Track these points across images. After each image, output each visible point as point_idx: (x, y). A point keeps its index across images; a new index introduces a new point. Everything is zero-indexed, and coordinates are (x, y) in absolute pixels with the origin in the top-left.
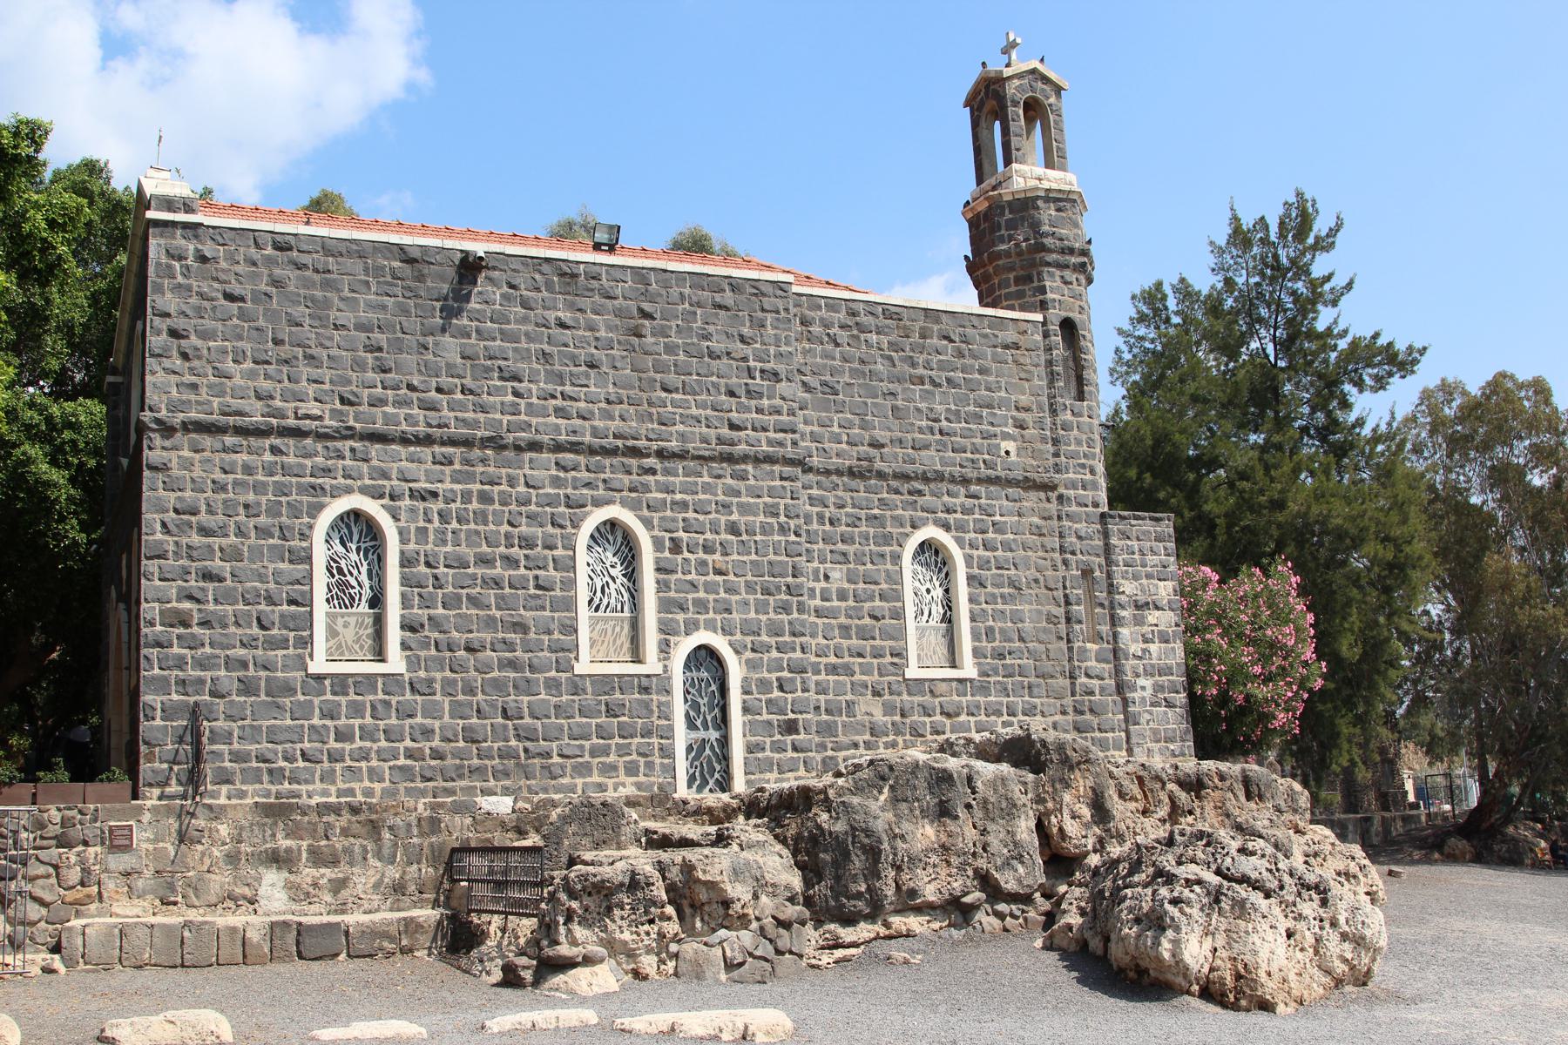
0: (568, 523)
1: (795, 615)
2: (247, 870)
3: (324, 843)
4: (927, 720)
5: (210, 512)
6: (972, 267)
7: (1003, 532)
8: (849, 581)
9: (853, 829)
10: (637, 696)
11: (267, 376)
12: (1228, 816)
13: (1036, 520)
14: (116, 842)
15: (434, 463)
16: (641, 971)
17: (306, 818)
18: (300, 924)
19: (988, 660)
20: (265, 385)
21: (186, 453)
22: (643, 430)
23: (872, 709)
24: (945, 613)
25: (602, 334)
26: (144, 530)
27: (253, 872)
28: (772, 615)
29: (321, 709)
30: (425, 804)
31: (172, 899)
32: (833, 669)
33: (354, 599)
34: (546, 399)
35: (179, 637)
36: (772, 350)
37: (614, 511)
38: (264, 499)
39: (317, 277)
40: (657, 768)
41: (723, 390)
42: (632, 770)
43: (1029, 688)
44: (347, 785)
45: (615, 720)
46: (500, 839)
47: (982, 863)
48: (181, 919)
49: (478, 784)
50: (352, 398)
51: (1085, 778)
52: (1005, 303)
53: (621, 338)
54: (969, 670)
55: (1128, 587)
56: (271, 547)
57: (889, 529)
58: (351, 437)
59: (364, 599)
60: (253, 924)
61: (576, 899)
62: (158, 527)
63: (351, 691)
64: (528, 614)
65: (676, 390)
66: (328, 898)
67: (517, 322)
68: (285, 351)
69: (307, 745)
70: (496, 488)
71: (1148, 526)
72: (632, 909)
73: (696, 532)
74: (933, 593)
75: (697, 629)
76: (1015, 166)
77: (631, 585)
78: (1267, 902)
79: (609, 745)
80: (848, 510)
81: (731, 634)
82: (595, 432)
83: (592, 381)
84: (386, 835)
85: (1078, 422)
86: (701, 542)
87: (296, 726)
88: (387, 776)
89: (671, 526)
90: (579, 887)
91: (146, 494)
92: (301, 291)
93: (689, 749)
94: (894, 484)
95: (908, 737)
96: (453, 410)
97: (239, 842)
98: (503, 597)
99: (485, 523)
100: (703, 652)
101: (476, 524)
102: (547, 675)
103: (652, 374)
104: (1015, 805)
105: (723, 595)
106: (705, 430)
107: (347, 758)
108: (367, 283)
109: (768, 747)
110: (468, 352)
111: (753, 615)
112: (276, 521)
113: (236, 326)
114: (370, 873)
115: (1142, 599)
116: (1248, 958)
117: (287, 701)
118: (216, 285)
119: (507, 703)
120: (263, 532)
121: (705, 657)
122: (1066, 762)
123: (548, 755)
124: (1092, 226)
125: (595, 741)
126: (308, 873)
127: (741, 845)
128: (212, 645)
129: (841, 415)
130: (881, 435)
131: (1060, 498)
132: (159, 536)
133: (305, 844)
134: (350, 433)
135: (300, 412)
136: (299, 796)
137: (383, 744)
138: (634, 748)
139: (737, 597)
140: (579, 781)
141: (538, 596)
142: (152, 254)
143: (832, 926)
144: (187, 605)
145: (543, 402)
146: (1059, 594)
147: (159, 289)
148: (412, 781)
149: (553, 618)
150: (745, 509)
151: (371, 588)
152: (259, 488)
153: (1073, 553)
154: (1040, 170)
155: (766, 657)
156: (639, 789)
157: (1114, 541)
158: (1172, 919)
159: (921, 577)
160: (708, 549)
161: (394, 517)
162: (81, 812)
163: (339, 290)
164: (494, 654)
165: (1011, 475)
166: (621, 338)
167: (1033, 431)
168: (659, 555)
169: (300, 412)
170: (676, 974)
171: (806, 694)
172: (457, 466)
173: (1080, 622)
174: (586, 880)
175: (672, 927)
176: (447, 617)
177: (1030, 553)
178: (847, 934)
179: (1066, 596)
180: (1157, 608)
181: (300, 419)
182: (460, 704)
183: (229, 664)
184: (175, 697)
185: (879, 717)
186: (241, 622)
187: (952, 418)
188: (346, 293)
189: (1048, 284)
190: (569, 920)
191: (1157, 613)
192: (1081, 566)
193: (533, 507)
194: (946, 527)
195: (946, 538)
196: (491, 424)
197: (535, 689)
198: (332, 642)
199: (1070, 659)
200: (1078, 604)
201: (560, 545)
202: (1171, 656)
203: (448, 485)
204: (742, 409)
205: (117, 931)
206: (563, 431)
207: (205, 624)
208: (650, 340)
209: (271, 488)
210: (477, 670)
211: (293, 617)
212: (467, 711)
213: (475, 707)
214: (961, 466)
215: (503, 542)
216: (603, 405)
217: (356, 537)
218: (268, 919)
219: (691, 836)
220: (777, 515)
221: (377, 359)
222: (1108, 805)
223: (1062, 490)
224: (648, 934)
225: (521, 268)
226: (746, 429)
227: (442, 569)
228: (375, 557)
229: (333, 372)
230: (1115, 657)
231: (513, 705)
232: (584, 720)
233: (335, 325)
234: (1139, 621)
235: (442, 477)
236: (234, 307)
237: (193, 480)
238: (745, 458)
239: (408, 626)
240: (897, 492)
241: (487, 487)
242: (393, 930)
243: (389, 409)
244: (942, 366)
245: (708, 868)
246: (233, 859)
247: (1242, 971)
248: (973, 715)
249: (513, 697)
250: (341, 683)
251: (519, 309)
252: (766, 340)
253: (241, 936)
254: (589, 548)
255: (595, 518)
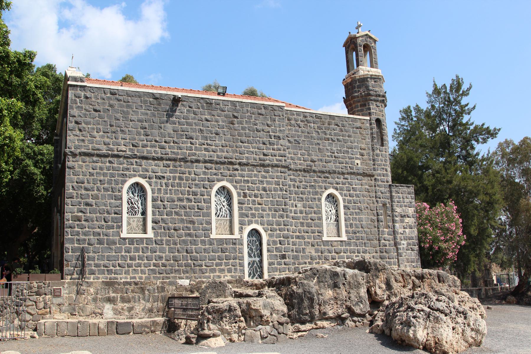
0: (209, 187)
1: (285, 219)
2: (100, 304)
3: (125, 295)
4: (330, 254)
5: (88, 183)
6: (345, 101)
7: (356, 191)
8: (303, 207)
9: (305, 291)
10: (232, 246)
11: (108, 137)
12: (432, 288)
13: (367, 187)
14: (56, 294)
15: (163, 167)
16: (232, 339)
17: (120, 286)
18: (117, 322)
19: (351, 234)
20: (107, 140)
21: (80, 163)
22: (234, 156)
23: (311, 251)
24: (336, 218)
25: (220, 123)
26: (66, 189)
27: (101, 304)
28: (277, 219)
29: (125, 249)
30: (160, 282)
31: (74, 313)
32: (298, 237)
33: (136, 212)
34: (201, 145)
35: (77, 225)
36: (278, 129)
37: (224, 183)
38: (106, 178)
39: (125, 104)
40: (238, 270)
41: (261, 142)
42: (230, 271)
43: (365, 244)
44: (133, 275)
45: (224, 254)
46: (185, 294)
47: (348, 303)
48: (77, 320)
49: (178, 275)
50: (136, 145)
51: (383, 275)
52: (357, 113)
53: (227, 125)
54: (344, 238)
55: (398, 210)
56: (109, 195)
57: (317, 190)
58: (136, 158)
59: (139, 212)
60: (101, 322)
61: (210, 315)
62: (71, 188)
63: (135, 243)
64: (195, 218)
65: (245, 142)
66: (127, 313)
67: (192, 119)
68: (114, 129)
69: (120, 262)
70: (184, 175)
71: (405, 189)
72: (230, 318)
73: (252, 190)
74: (332, 211)
75: (252, 223)
76: (360, 67)
77: (230, 208)
78: (446, 317)
79: (222, 263)
80: (303, 183)
81: (264, 225)
82: (218, 157)
83: (217, 139)
84: (147, 292)
85: (381, 154)
86: (253, 194)
87: (117, 255)
88: (147, 272)
89: (243, 188)
90: (211, 310)
91: (67, 177)
92: (119, 109)
93: (249, 264)
94: (319, 174)
95: (323, 260)
96: (170, 149)
97: (97, 294)
98: (186, 212)
99: (181, 187)
100: (254, 231)
101: (178, 187)
102: (201, 239)
103: (237, 137)
104: (360, 284)
105: (261, 212)
106: (255, 156)
107: (134, 266)
108: (142, 106)
109: (276, 263)
110: (175, 129)
111: (271, 219)
112: (110, 186)
113: (98, 120)
114: (141, 305)
115: (403, 214)
116: (439, 337)
117: (114, 247)
118: (91, 106)
119: (187, 248)
120: (106, 190)
121: (255, 233)
122: (377, 269)
123: (201, 266)
124: (386, 87)
125: (217, 261)
126: (120, 305)
127: (266, 297)
128: (88, 228)
129: (301, 151)
130: (315, 158)
131: (375, 179)
132: (71, 191)
133: (119, 295)
134: (135, 157)
135: (119, 149)
136: (117, 279)
137: (146, 261)
138: (230, 263)
139: (266, 213)
140: (212, 275)
141: (198, 212)
142: (69, 96)
143: (297, 325)
144: (80, 214)
145: (200, 146)
146: (375, 212)
147: (72, 108)
148: (156, 274)
149: (203, 219)
150: (268, 183)
151: (142, 209)
152: (105, 175)
153: (380, 198)
154: (369, 68)
155: (275, 233)
156: (232, 277)
157: (393, 194)
158: (413, 323)
159: (328, 206)
160: (256, 196)
161: (150, 185)
162: (44, 284)
163: (132, 108)
164: (183, 231)
165: (359, 172)
166: (227, 125)
167: (366, 157)
168: (239, 198)
169: (119, 149)
170: (244, 340)
171: (289, 246)
172: (171, 168)
173: (382, 222)
174: (214, 308)
175: (243, 325)
176: (168, 219)
177: (365, 198)
178: (302, 327)
179: (377, 213)
180: (408, 217)
181: (119, 151)
182: (172, 248)
183: (94, 234)
184: (76, 245)
185: (314, 254)
186: (98, 220)
187: (339, 152)
188: (134, 109)
189: (371, 107)
190: (208, 322)
191: (408, 219)
192: (382, 203)
193: (197, 182)
194: (337, 189)
195: (336, 193)
196: (183, 154)
197: (197, 243)
198: (129, 227)
199: (379, 234)
200: (381, 216)
201: (206, 194)
202: (413, 233)
203: (168, 174)
204: (268, 149)
205: (56, 324)
206: (207, 156)
207: (86, 220)
208: (236, 125)
209: (109, 175)
210: (177, 237)
211: (116, 218)
212: (174, 251)
213: (177, 249)
214: (342, 168)
215: (187, 194)
216: (221, 147)
217: (137, 192)
218: (107, 321)
219: (249, 293)
220: (279, 185)
221: (144, 131)
222: (391, 284)
223: (376, 177)
224: (235, 327)
225: (193, 101)
226: (269, 156)
227: (166, 203)
228: (143, 198)
229: (130, 136)
230: (394, 233)
231: (190, 249)
232: (214, 254)
233: (130, 120)
234: (402, 221)
235: (166, 171)
236: (97, 114)
237: (83, 172)
238: (268, 166)
239: (154, 222)
240: (320, 177)
241: (181, 175)
242: (149, 325)
243: (149, 148)
244: (335, 135)
245: (255, 304)
246: (95, 300)
247: (437, 341)
248: (345, 253)
249: (189, 246)
250: (132, 241)
251: (192, 115)
252: (276, 126)
253: (97, 326)
254: (216, 195)
255: (218, 185)
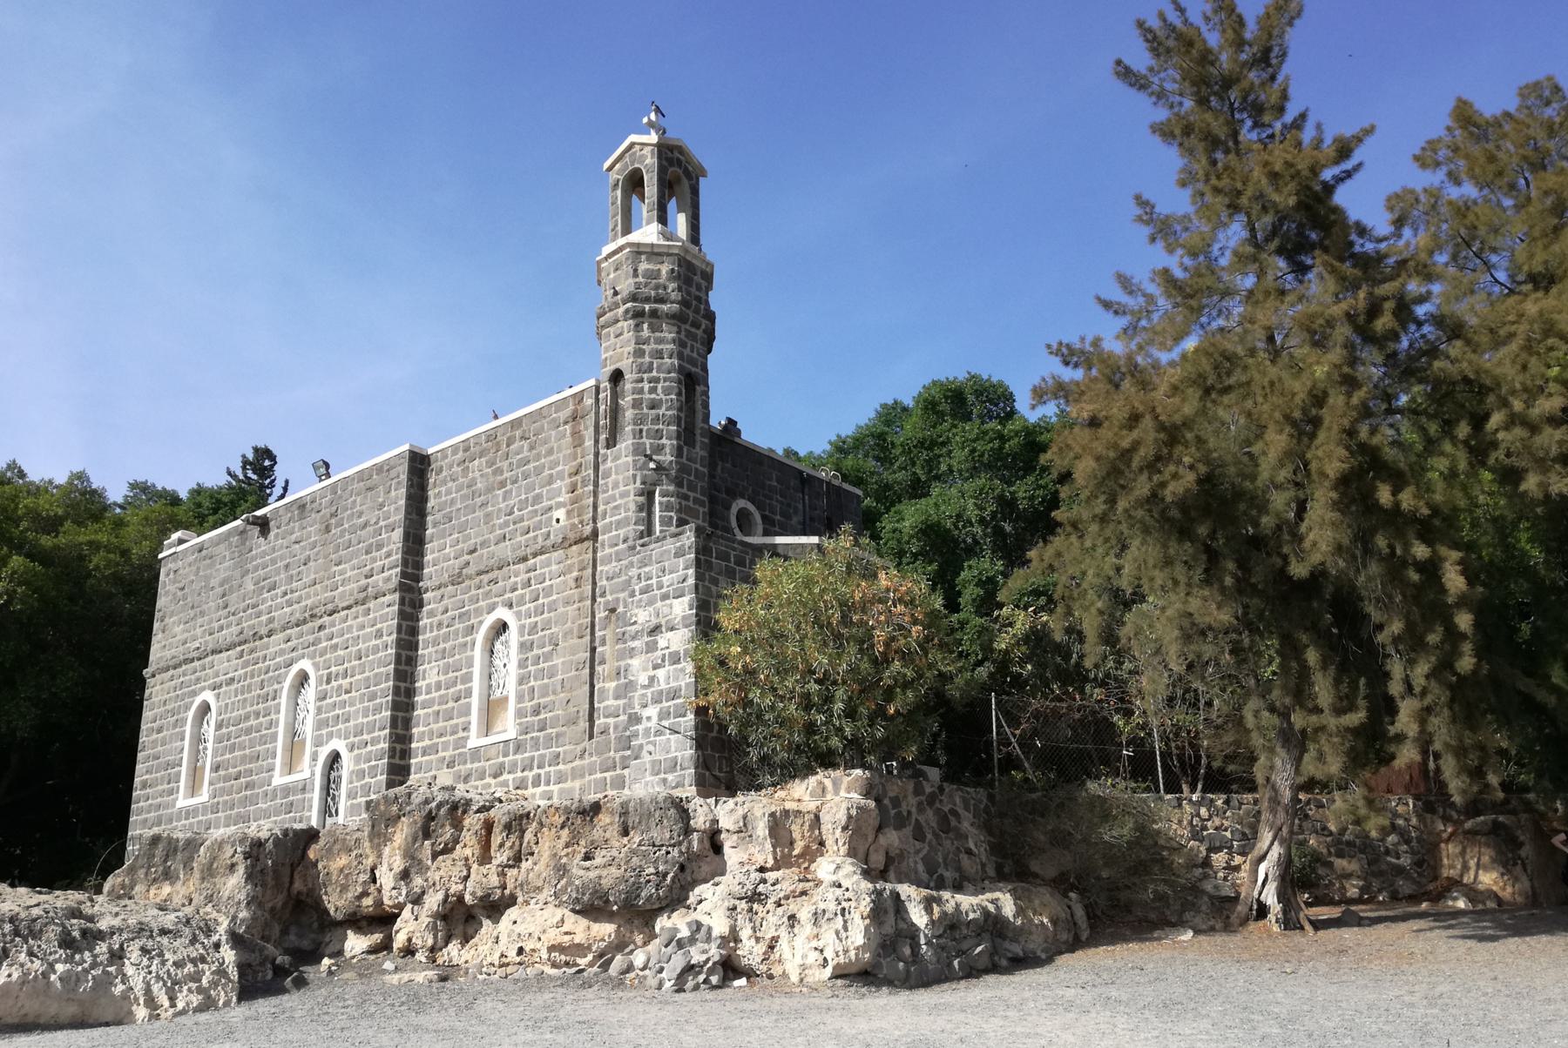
115: (654, 621)
191: (670, 634)
234: (651, 647)
